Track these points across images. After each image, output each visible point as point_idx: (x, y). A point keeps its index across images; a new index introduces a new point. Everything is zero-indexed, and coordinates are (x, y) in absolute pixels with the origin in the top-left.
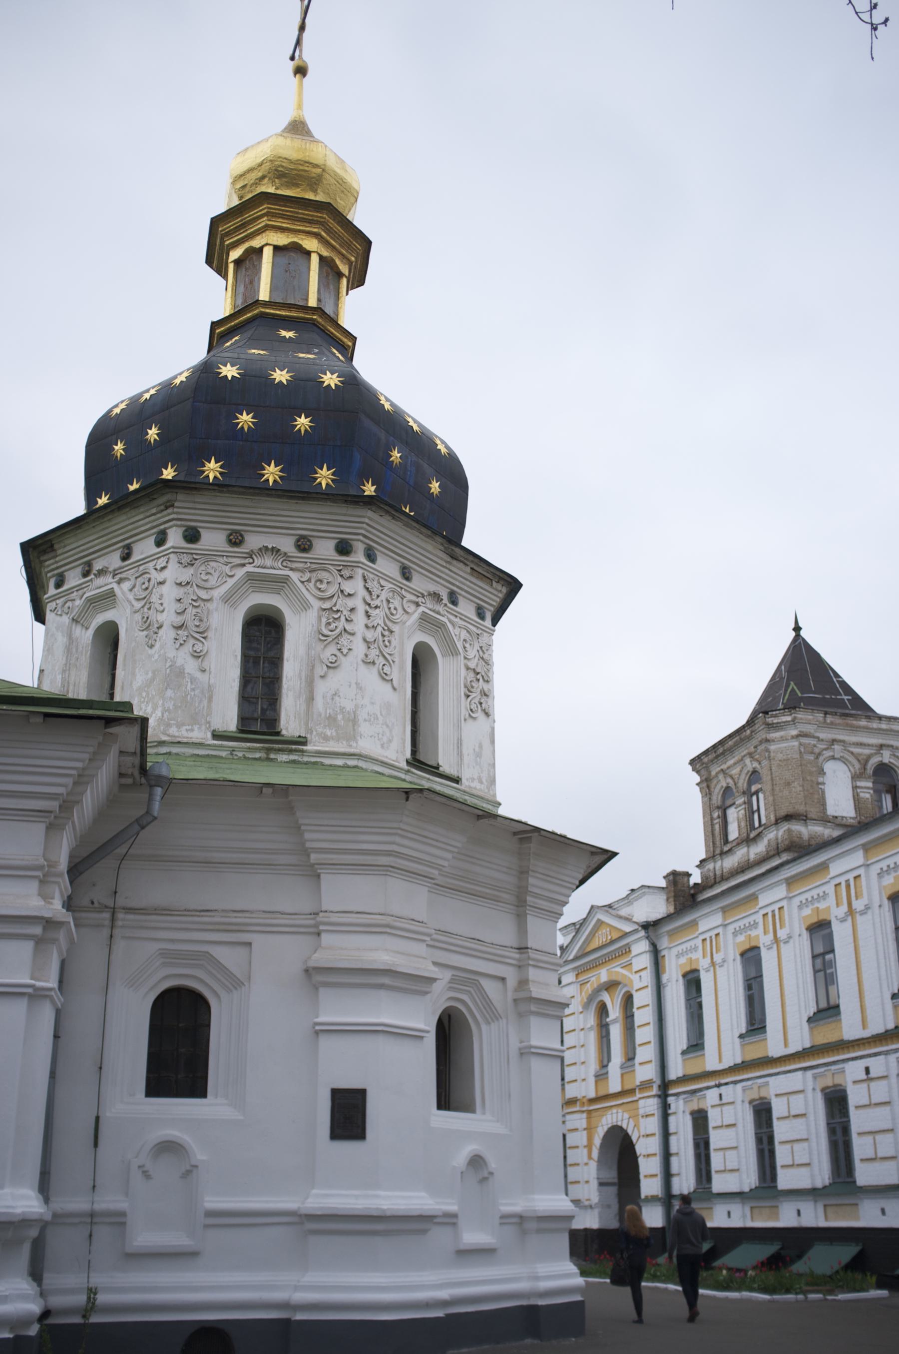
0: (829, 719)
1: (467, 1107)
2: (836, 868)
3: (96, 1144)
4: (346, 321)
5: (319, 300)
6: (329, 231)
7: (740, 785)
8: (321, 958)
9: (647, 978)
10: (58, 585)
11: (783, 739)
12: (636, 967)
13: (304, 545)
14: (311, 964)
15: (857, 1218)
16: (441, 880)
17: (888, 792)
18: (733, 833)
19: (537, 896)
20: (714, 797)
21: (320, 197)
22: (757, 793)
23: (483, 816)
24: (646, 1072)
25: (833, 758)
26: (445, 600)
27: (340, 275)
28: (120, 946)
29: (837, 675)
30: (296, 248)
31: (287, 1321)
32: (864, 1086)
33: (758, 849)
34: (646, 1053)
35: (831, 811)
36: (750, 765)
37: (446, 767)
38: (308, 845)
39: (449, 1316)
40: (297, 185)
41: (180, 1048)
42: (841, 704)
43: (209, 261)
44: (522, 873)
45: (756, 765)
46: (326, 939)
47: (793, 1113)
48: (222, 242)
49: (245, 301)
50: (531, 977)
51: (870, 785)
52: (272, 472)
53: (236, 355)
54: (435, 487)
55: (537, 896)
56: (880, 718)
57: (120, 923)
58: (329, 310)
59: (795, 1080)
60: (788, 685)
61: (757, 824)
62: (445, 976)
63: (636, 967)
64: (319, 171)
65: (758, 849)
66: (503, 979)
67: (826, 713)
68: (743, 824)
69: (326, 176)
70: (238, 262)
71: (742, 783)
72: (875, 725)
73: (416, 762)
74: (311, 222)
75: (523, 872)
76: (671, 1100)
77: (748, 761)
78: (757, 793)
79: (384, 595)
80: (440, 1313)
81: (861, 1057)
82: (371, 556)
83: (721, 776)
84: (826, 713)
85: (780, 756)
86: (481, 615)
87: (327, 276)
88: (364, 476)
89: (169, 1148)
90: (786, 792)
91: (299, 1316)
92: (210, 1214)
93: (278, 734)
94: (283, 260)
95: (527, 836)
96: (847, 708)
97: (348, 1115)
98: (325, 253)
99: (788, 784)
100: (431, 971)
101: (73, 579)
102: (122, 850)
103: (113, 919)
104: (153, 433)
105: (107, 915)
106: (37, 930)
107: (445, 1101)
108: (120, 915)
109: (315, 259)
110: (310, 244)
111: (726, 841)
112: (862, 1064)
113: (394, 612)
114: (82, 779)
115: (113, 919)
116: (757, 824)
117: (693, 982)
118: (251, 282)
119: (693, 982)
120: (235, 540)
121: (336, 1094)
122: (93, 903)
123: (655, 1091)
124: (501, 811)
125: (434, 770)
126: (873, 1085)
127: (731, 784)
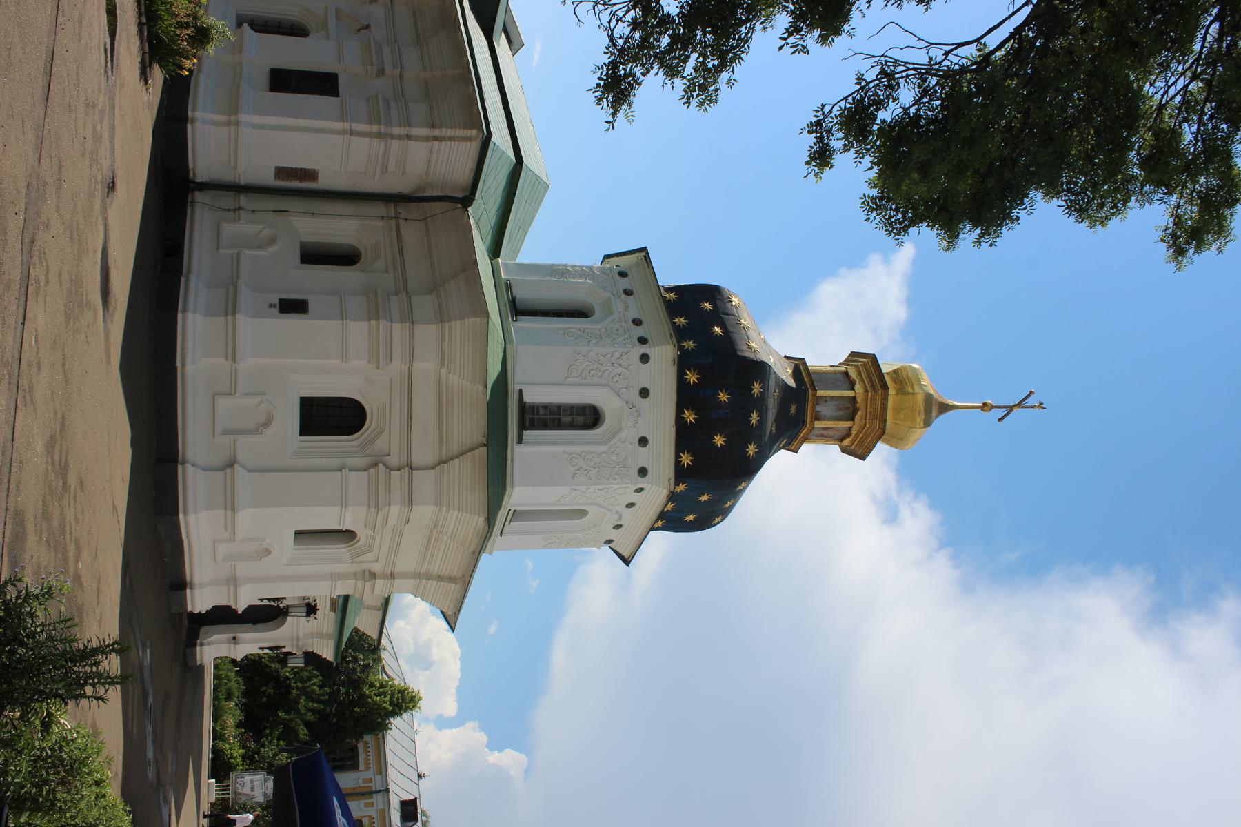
5: (826, 399)
6: (873, 399)
13: (637, 322)
27: (852, 419)
28: (380, 223)
31: (181, 273)
39: (175, 368)
52: (681, 321)
74: (873, 386)
79: (620, 370)
87: (848, 408)
88: (698, 369)
92: (239, 254)
94: (841, 378)
97: (293, 307)
98: (859, 400)
109: (851, 393)
110: (858, 387)
113: (616, 378)
115: (392, 218)
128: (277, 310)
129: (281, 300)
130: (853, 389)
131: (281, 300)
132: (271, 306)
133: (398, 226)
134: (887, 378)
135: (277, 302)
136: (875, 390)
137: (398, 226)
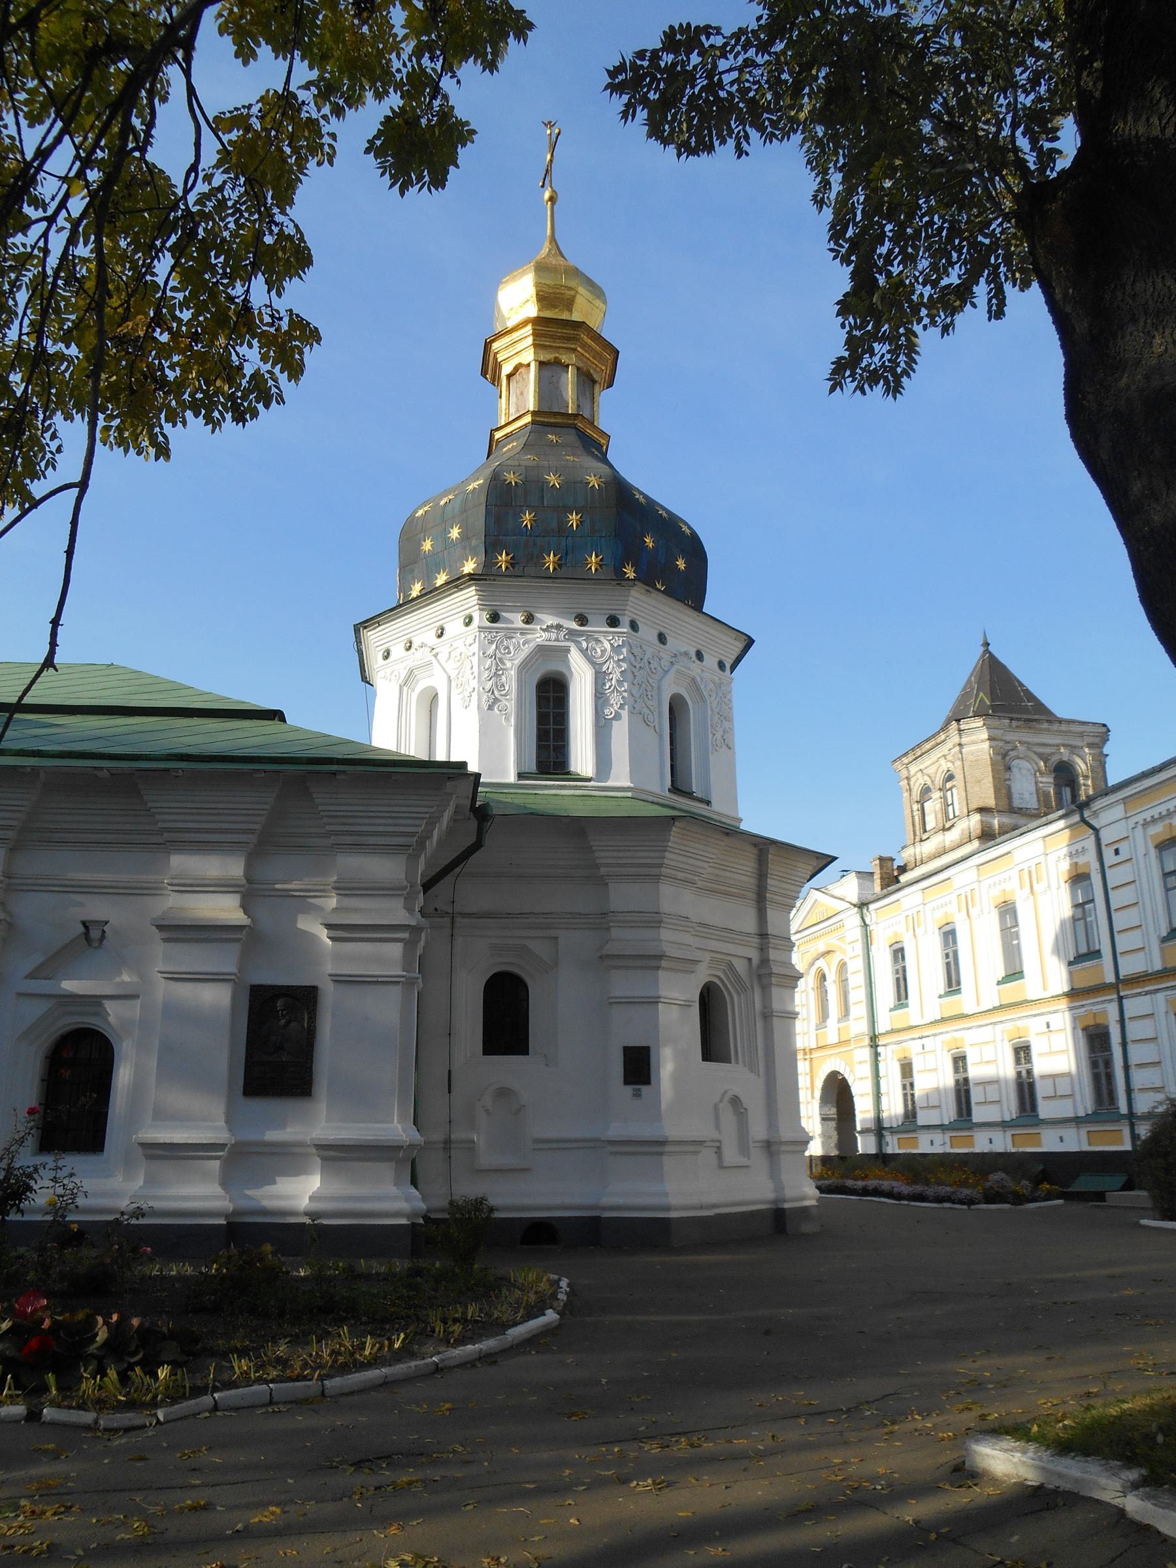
0: (1014, 723)
1: (724, 1058)
2: (1018, 856)
3: (450, 1092)
4: (603, 423)
5: (579, 406)
7: (936, 782)
8: (610, 949)
9: (859, 947)
10: (387, 655)
11: (973, 743)
12: (849, 939)
14: (604, 952)
15: (1039, 1145)
16: (700, 884)
17: (1067, 785)
18: (931, 823)
19: (775, 893)
20: (914, 793)
21: (576, 317)
22: (951, 789)
23: (730, 832)
24: (862, 1027)
25: (1018, 758)
26: (694, 658)
28: (459, 942)
29: (1021, 685)
30: (557, 363)
32: (1045, 1038)
33: (953, 836)
34: (859, 1010)
35: (1017, 803)
36: (945, 765)
37: (698, 794)
38: (598, 861)
40: (555, 307)
41: (507, 1020)
42: (1025, 710)
43: (484, 373)
44: (760, 875)
45: (950, 765)
46: (615, 933)
47: (985, 1059)
48: (495, 359)
49: (518, 410)
50: (771, 957)
51: (1051, 780)
53: (517, 463)
54: (681, 564)
55: (775, 893)
56: (1060, 721)
57: (457, 925)
58: (587, 414)
59: (986, 1033)
60: (977, 695)
61: (951, 816)
62: (707, 956)
63: (849, 940)
64: (573, 293)
65: (953, 836)
66: (750, 959)
67: (1011, 719)
68: (940, 816)
69: (578, 297)
70: (509, 376)
71: (939, 781)
72: (1055, 727)
73: (675, 789)
74: (569, 339)
75: (762, 876)
76: (880, 1049)
77: (942, 761)
78: (951, 789)
80: (711, 1213)
81: (1042, 1014)
82: (634, 626)
83: (920, 774)
84: (1011, 719)
85: (971, 758)
86: (721, 665)
89: (504, 1093)
90: (977, 789)
91: (606, 1214)
93: (568, 773)
94: (547, 373)
95: (764, 848)
96: (1029, 713)
97: (638, 1066)
98: (581, 365)
99: (979, 781)
100: (698, 955)
101: (398, 651)
102: (457, 870)
103: (453, 923)
104: (455, 533)
105: (447, 920)
106: (406, 935)
107: (708, 1055)
108: (458, 920)
111: (925, 831)
112: (1042, 1020)
114: (433, 821)
115: (453, 923)
116: (951, 816)
117: (899, 953)
118: (522, 394)
119: (899, 953)
120: (529, 619)
121: (627, 1050)
122: (436, 909)
123: (867, 1041)
124: (744, 826)
125: (689, 795)
126: (1053, 1036)
127: (929, 783)
128: (644, 1089)
129: (627, 1082)
130: (567, 366)
131: (627, 1082)
132: (637, 1095)
133: (465, 915)
134: (548, 314)
135: (629, 1089)
136: (575, 339)
137: (465, 915)
